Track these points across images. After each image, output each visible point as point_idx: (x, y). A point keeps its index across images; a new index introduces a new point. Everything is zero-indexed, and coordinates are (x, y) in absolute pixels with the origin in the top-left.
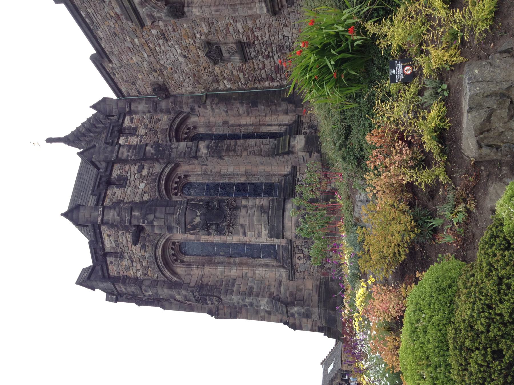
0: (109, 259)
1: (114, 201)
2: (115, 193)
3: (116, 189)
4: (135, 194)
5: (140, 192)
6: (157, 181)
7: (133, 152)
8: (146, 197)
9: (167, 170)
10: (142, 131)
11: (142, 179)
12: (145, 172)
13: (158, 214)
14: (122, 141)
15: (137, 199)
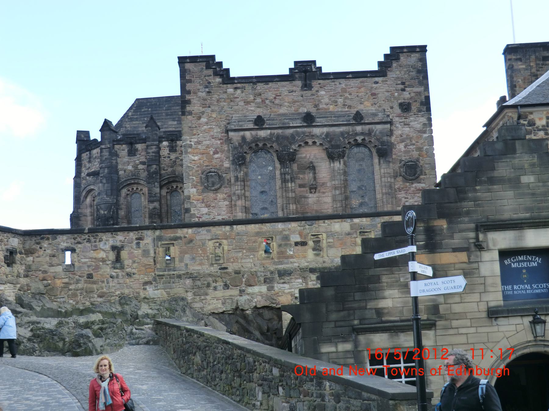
0: (88, 153)
1: (118, 151)
2: (123, 150)
3: (126, 150)
4: (124, 164)
5: (125, 167)
6: (134, 177)
7: (152, 156)
8: (121, 173)
9: (142, 182)
10: (173, 156)
11: (135, 167)
12: (141, 167)
13: (106, 185)
14: (165, 143)
15: (120, 167)
